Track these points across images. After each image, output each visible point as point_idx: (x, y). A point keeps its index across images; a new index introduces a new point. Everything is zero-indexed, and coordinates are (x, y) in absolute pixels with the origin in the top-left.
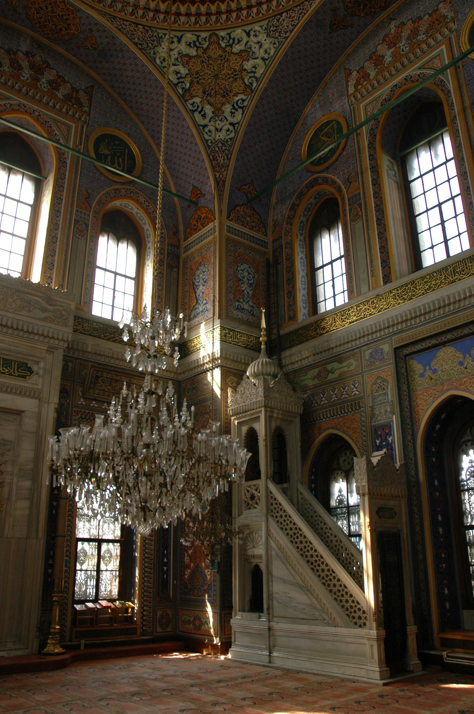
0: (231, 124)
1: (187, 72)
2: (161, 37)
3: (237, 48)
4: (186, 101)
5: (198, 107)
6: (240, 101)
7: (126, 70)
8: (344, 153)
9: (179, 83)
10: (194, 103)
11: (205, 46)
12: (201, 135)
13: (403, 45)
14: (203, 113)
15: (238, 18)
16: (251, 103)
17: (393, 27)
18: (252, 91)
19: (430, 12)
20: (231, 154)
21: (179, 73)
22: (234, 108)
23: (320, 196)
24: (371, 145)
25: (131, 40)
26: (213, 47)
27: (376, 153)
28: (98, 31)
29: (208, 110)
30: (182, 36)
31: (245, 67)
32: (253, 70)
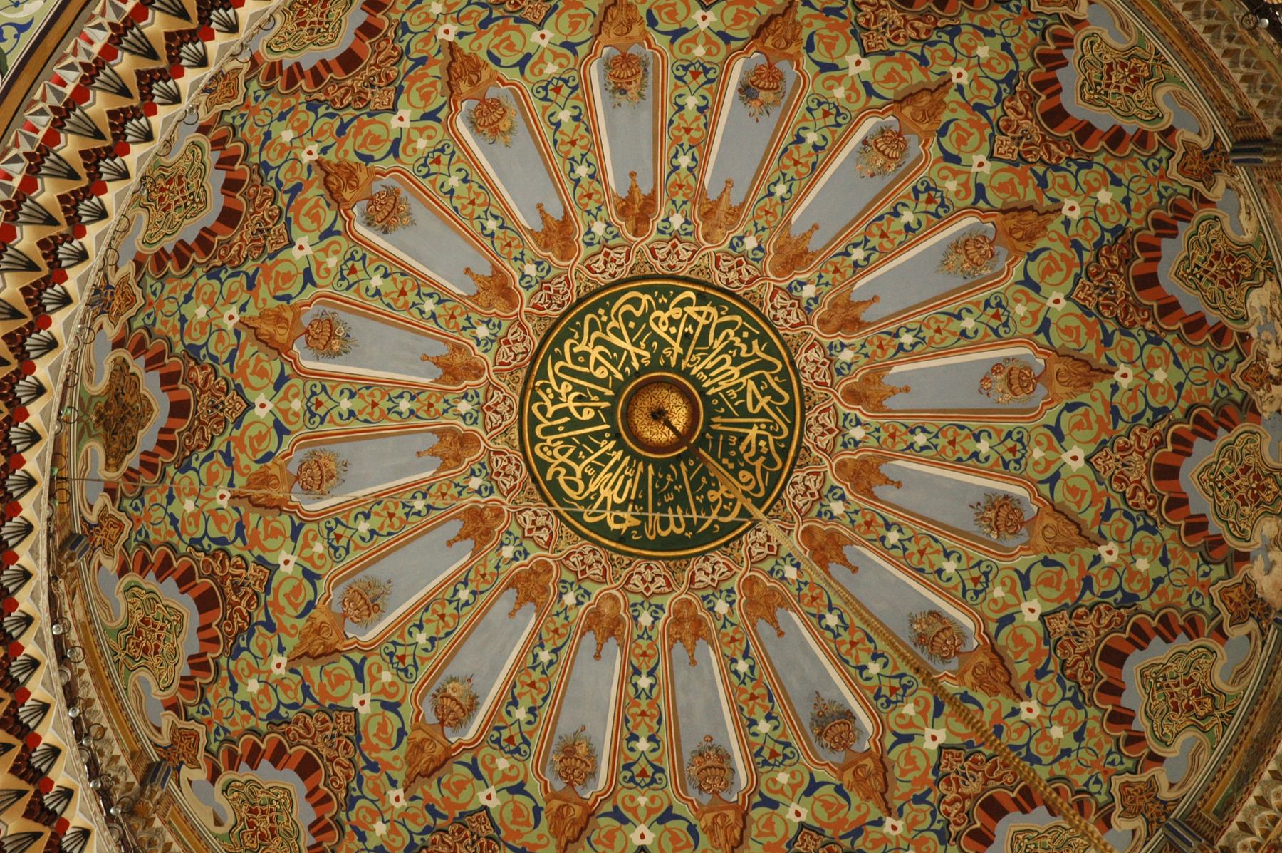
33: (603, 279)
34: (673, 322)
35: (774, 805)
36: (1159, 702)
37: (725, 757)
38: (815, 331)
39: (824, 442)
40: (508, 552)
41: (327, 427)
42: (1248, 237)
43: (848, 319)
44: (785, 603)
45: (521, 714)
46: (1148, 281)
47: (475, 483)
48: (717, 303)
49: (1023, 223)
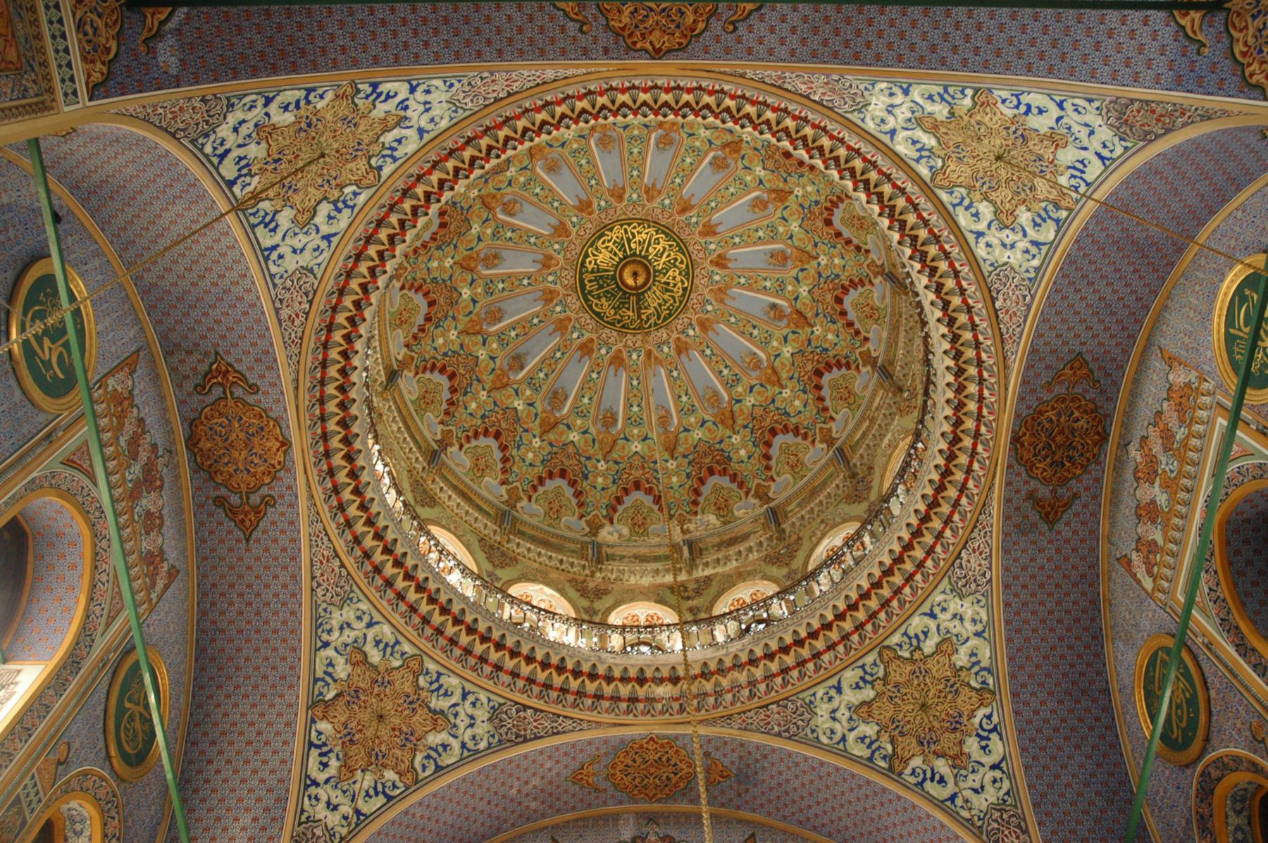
0: (995, 767)
1: (876, 728)
2: (811, 702)
3: (929, 646)
4: (900, 774)
5: (924, 772)
6: (985, 720)
7: (787, 781)
8: (1213, 693)
9: (873, 753)
10: (914, 770)
11: (881, 674)
12: (954, 816)
13: (1167, 464)
14: (937, 777)
15: (902, 604)
16: (1001, 711)
17: (1135, 454)
18: (994, 693)
19: (1165, 396)
20: (1024, 820)
21: (865, 737)
22: (982, 738)
23: (1243, 801)
24: (1243, 648)
25: (768, 733)
26: (893, 666)
27: (1261, 656)
28: (717, 749)
29: (942, 766)
30: (839, 682)
31: (959, 664)
32: (974, 659)
33: (691, 249)
34: (674, 278)
35: (484, 344)
36: (551, 496)
37: (500, 320)
38: (675, 336)
39: (629, 343)
40: (574, 219)
41: (626, 144)
42: (736, 513)
43: (681, 349)
44: (563, 334)
45: (509, 234)
46: (711, 472)
47: (603, 203)
48: (683, 295)
49: (728, 419)
